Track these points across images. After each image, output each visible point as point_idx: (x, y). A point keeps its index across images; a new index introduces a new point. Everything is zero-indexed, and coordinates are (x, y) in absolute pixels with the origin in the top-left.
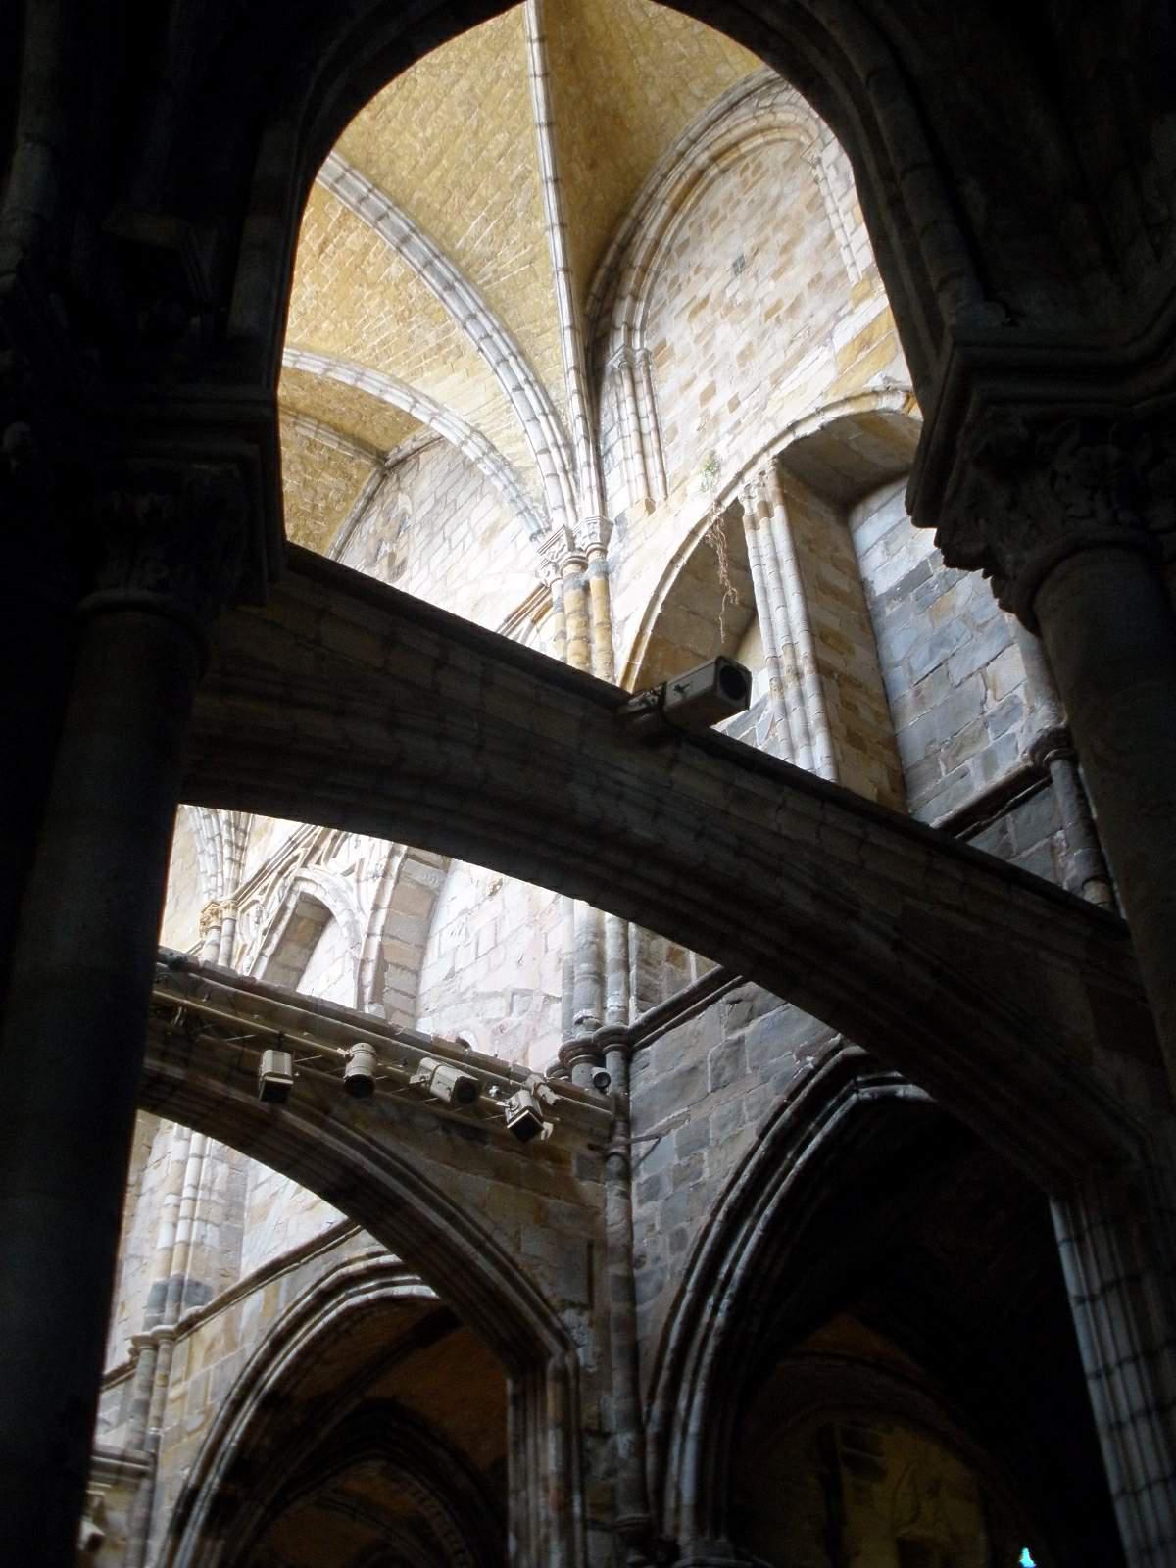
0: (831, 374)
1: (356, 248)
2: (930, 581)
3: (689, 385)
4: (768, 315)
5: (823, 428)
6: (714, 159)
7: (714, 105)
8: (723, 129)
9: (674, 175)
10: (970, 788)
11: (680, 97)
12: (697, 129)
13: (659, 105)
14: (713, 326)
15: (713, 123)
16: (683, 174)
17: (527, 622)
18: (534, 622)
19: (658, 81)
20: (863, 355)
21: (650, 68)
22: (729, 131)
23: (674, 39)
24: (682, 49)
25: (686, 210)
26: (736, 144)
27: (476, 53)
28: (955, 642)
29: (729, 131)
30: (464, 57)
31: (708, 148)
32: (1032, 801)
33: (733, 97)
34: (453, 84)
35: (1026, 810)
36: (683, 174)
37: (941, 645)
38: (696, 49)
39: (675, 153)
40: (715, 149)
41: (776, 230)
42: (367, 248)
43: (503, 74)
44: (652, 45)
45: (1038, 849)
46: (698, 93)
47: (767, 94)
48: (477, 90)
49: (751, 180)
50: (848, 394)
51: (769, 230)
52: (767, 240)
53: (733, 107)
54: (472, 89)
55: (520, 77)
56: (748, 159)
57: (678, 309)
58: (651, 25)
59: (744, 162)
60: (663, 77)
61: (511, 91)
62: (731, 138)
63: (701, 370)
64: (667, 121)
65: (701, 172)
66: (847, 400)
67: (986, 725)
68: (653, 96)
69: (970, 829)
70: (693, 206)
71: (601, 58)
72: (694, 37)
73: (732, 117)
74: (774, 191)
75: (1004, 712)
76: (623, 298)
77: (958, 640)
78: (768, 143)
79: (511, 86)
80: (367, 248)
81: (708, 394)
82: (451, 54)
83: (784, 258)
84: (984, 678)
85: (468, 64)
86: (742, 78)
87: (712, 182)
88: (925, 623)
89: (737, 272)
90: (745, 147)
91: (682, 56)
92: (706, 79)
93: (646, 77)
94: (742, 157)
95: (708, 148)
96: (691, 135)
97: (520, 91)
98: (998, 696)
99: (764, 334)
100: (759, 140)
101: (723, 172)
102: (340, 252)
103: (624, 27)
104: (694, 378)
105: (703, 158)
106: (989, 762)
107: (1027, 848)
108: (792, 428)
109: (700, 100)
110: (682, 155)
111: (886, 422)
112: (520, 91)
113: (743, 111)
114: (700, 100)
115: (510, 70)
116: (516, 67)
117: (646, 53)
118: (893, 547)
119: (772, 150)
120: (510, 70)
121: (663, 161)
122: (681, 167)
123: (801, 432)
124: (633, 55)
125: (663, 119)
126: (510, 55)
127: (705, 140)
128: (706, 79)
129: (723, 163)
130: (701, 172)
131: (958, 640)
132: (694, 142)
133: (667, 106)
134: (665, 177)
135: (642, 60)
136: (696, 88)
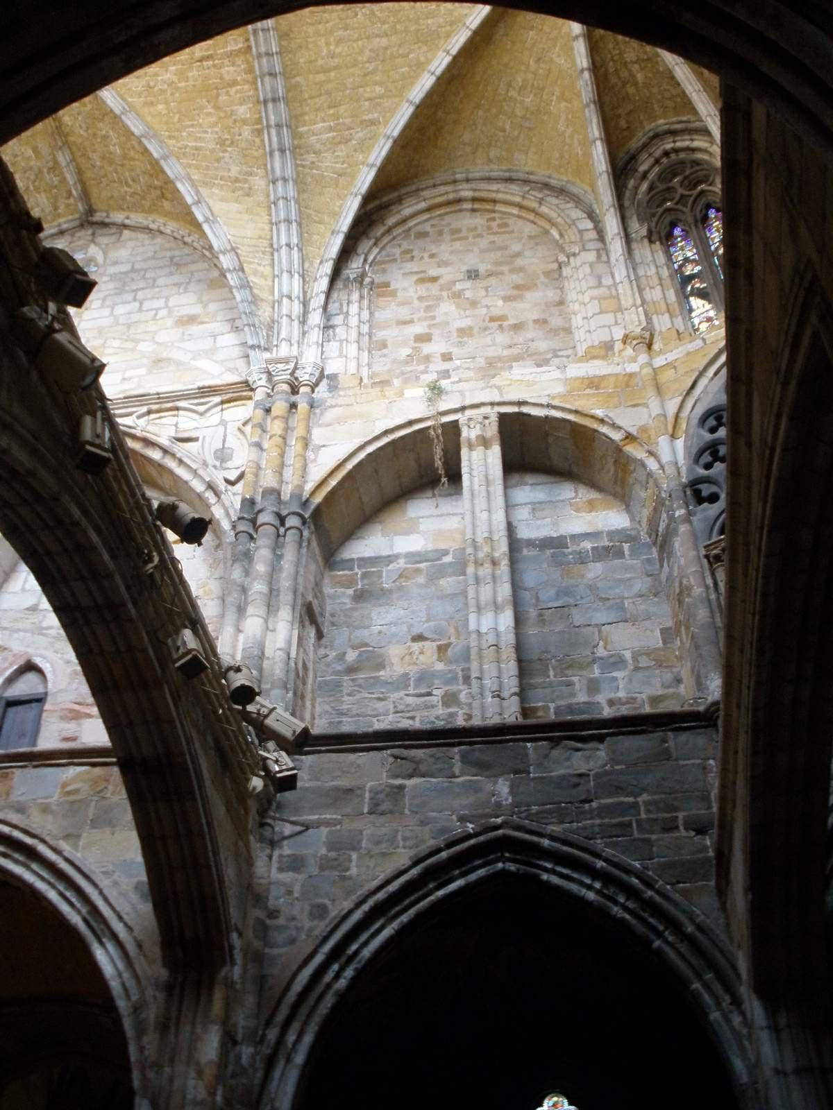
0: (559, 389)
1: (227, 77)
2: (566, 551)
3: (405, 323)
4: (492, 319)
5: (547, 417)
6: (474, 200)
7: (496, 170)
8: (495, 187)
9: (443, 189)
10: (573, 695)
11: (480, 150)
12: (478, 175)
13: (464, 144)
14: (439, 298)
15: (489, 179)
16: (447, 193)
17: (217, 399)
18: (223, 402)
19: (478, 132)
20: (589, 391)
22: (498, 191)
23: (509, 118)
25: (434, 214)
26: (495, 201)
27: (406, 31)
28: (578, 598)
29: (498, 191)
30: (398, 27)
31: (475, 190)
32: (692, 732)
33: (514, 175)
34: (378, 36)
35: (684, 737)
36: (447, 193)
37: (567, 594)
38: (516, 133)
39: (452, 178)
40: (477, 194)
41: (512, 271)
42: (234, 83)
43: (411, 56)
44: (494, 111)
45: (693, 764)
47: (541, 190)
48: (389, 52)
49: (496, 229)
50: (579, 409)
51: (505, 268)
52: (502, 273)
53: (510, 180)
54: (386, 48)
55: (420, 66)
56: (497, 215)
57: (407, 271)
58: (504, 100)
59: (493, 215)
60: (482, 132)
61: (407, 69)
62: (500, 196)
63: (420, 319)
64: (461, 156)
65: (459, 201)
66: (576, 412)
67: (594, 661)
68: (467, 137)
69: (639, 728)
70: (439, 215)
71: (462, 93)
72: (521, 126)
73: (507, 185)
74: (516, 247)
75: (612, 660)
76: (368, 237)
77: (582, 598)
78: (519, 217)
79: (410, 67)
80: (234, 83)
81: (425, 338)
82: (392, 19)
83: (515, 292)
84: (600, 631)
85: (396, 33)
86: (527, 169)
87: (460, 211)
88: (556, 574)
89: (469, 277)
90: (499, 207)
91: (504, 131)
92: (504, 153)
94: (494, 211)
95: (475, 190)
96: (471, 176)
97: (412, 74)
98: (609, 647)
99: (486, 329)
100: (515, 211)
101: (473, 210)
102: (213, 71)
103: (489, 89)
104: (411, 322)
105: (468, 194)
106: (593, 686)
107: (685, 759)
108: (520, 403)
109: (490, 161)
110: (455, 182)
111: (594, 441)
112: (412, 74)
113: (514, 187)
114: (490, 161)
115: (418, 58)
116: (422, 59)
118: (538, 514)
119: (520, 223)
120: (418, 58)
121: (440, 176)
122: (449, 188)
123: (525, 409)
124: (478, 107)
125: (459, 153)
126: (425, 49)
127: (473, 185)
128: (504, 153)
129: (477, 206)
130: (459, 201)
131: (582, 598)
132: (468, 180)
133: (468, 149)
134: (435, 186)
135: (480, 113)
136: (493, 153)
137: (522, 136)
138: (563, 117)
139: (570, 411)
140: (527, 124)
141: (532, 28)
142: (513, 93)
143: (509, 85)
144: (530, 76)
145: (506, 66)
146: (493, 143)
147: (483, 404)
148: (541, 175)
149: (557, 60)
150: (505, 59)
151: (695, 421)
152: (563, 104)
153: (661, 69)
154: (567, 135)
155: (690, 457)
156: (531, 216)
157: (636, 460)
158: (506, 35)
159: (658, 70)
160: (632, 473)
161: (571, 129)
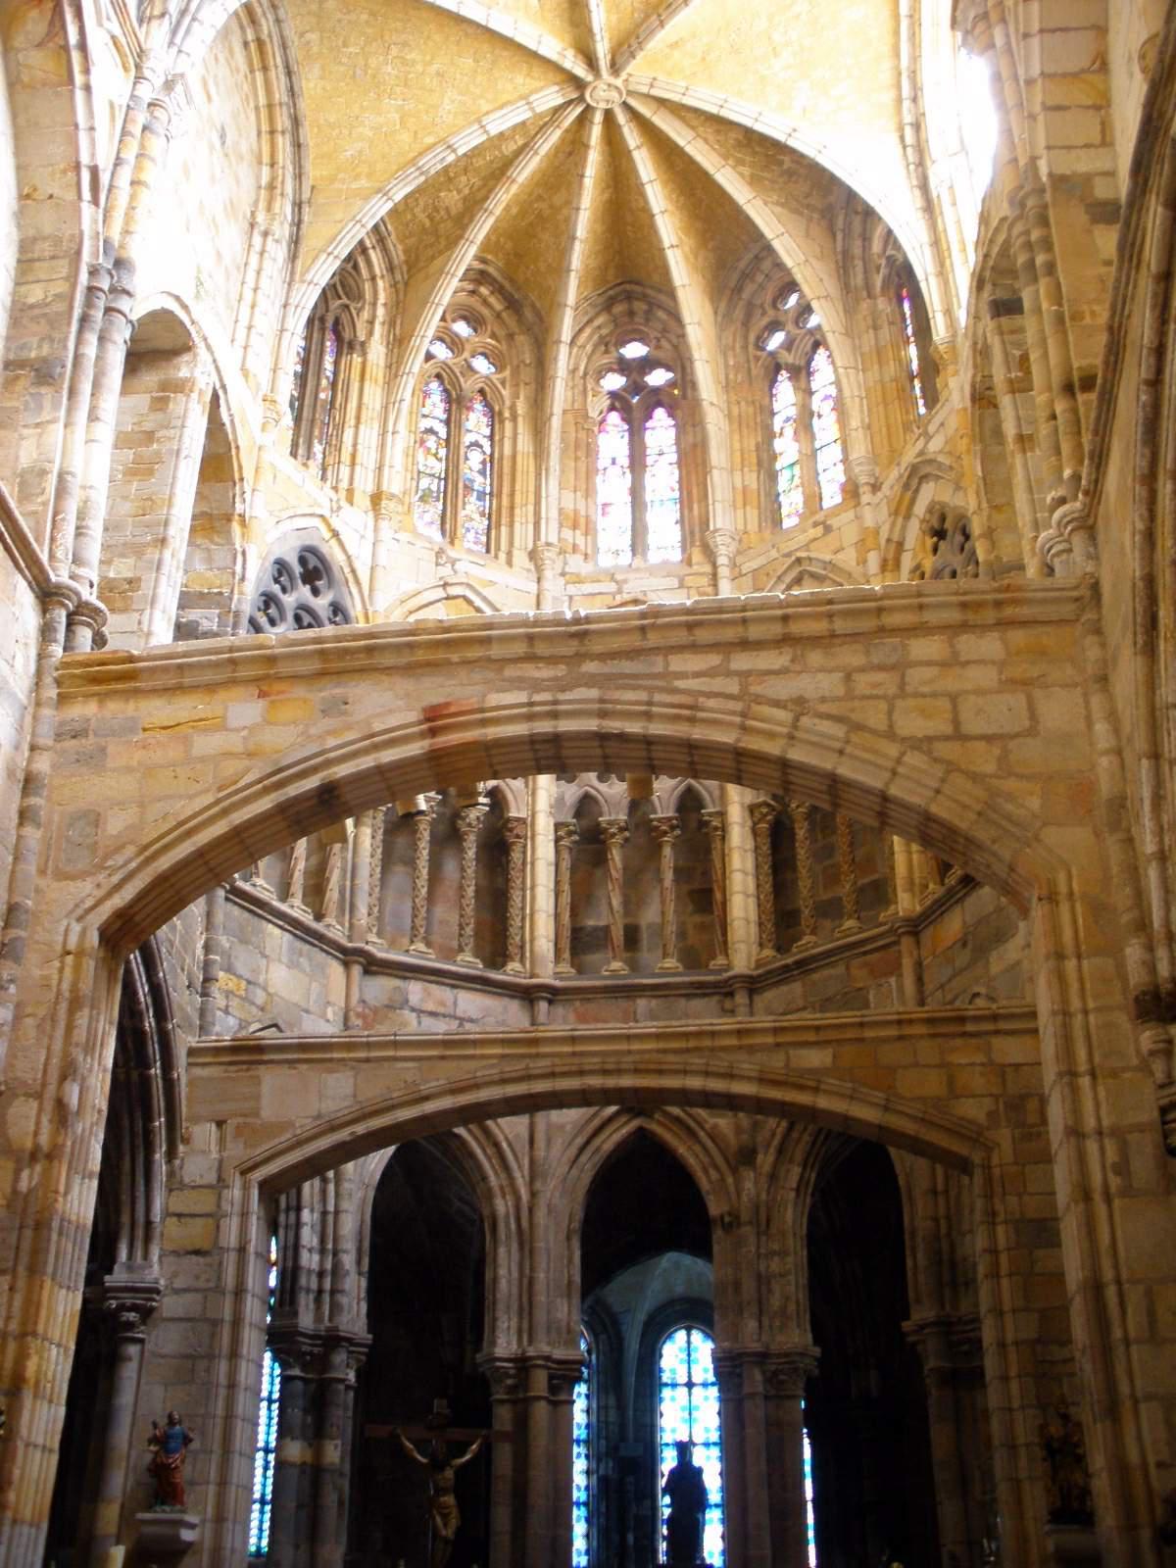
6: (260, 43)
12: (287, 33)
15: (284, 47)
17: (118, 32)
18: (113, 38)
19: (339, 16)
21: (353, 17)
24: (351, 49)
38: (344, 60)
44: (369, 31)
46: (309, 36)
53: (289, 73)
66: (237, 448)
78: (257, 108)
90: (259, 75)
91: (345, 45)
93: (349, 12)
100: (262, 101)
109: (302, 35)
117: (367, 22)
124: (373, 14)
128: (315, 49)
129: (253, 46)
135: (364, 17)
137: (342, 69)
138: (381, 120)
139: (236, 440)
140: (358, 72)
141: (476, 61)
142: (394, 51)
143: (405, 44)
144: (419, 67)
145: (429, 37)
146: (326, 35)
147: (212, 353)
148: (304, 105)
149: (446, 101)
150: (437, 37)
151: (272, 559)
152: (397, 116)
153: (442, 194)
154: (361, 129)
155: (257, 589)
156: (265, 127)
157: (230, 542)
158: (467, 35)
159: (440, 191)
160: (212, 541)
161: (371, 134)
